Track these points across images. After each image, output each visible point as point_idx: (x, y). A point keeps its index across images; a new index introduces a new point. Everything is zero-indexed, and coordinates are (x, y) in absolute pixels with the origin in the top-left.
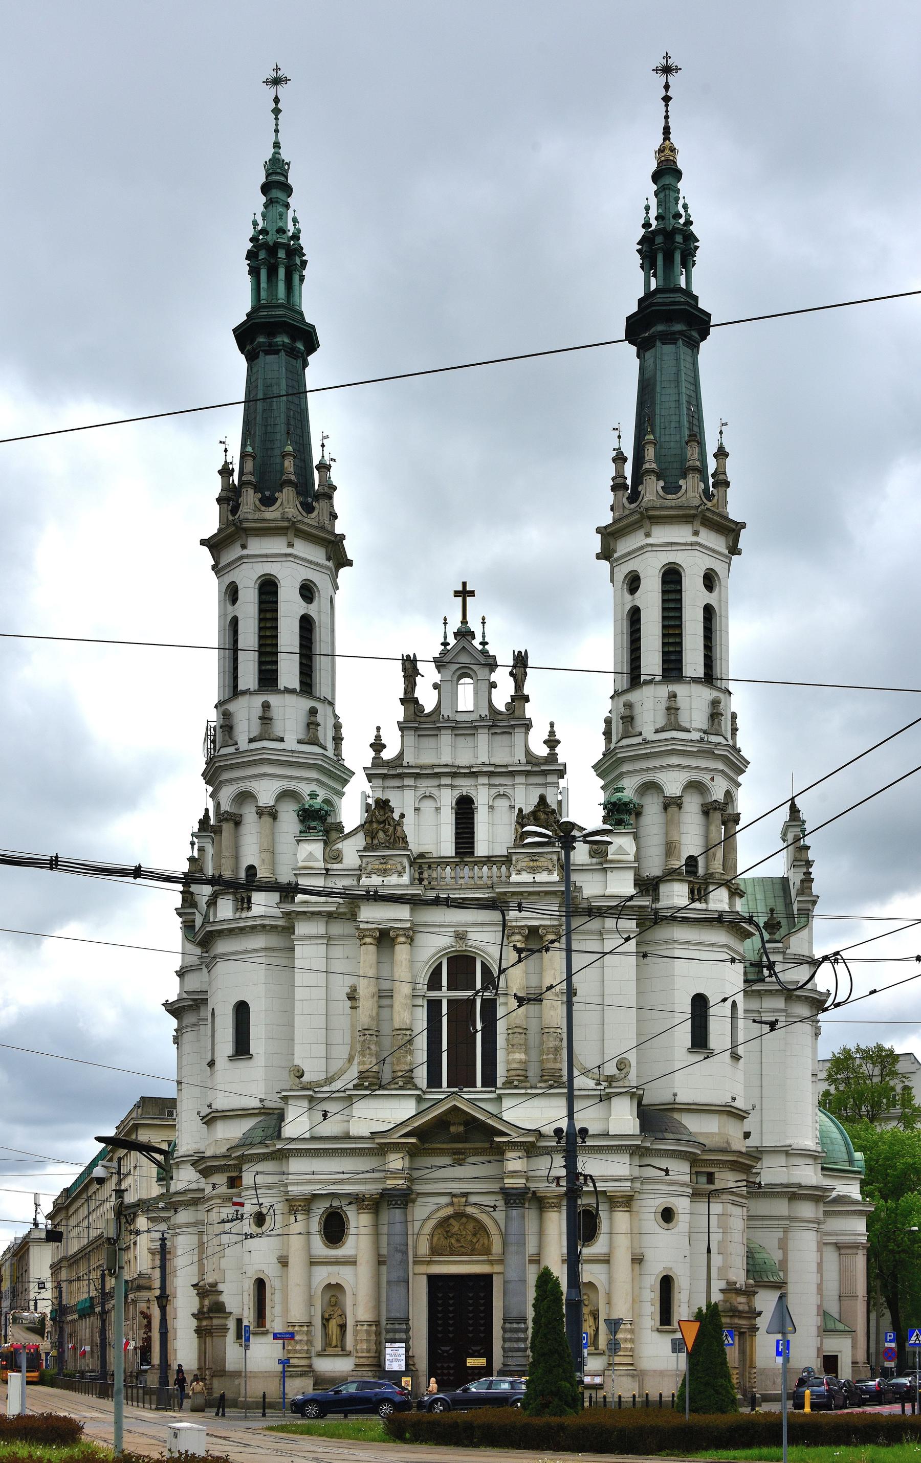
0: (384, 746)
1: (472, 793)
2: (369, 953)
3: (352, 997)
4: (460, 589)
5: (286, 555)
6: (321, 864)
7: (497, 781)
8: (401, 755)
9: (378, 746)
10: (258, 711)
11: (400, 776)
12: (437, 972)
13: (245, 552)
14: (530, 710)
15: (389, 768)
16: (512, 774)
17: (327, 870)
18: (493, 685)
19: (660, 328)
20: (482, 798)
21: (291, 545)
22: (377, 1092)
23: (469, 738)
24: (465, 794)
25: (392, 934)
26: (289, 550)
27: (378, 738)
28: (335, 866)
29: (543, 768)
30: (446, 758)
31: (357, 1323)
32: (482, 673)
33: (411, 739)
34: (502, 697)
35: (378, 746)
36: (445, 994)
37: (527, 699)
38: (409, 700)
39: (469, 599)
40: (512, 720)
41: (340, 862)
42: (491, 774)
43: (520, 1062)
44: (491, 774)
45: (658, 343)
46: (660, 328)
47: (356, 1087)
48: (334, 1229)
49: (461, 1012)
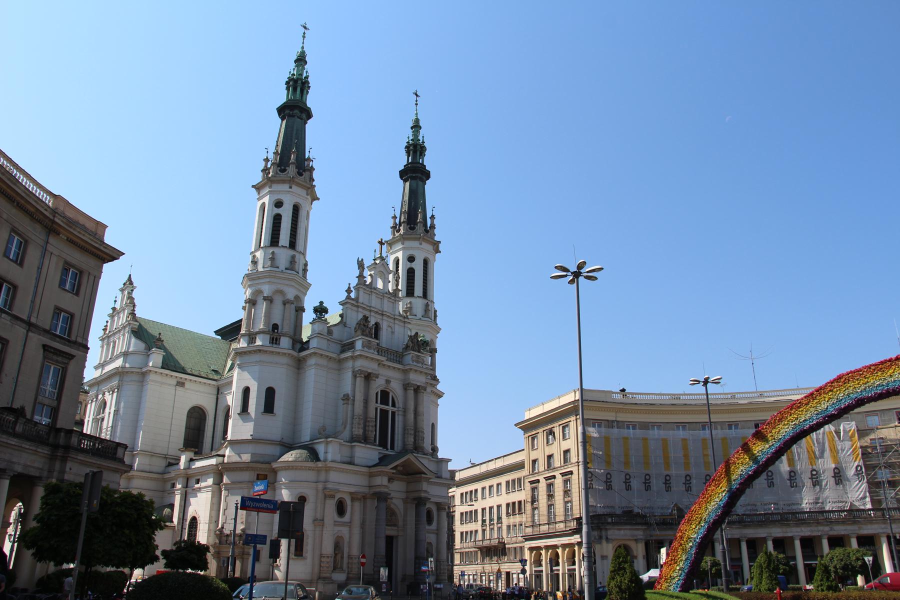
9: (349, 291)
10: (289, 259)
11: (358, 306)
27: (349, 288)
31: (350, 557)
34: (391, 287)
38: (361, 277)
48: (341, 509)
49: (384, 413)
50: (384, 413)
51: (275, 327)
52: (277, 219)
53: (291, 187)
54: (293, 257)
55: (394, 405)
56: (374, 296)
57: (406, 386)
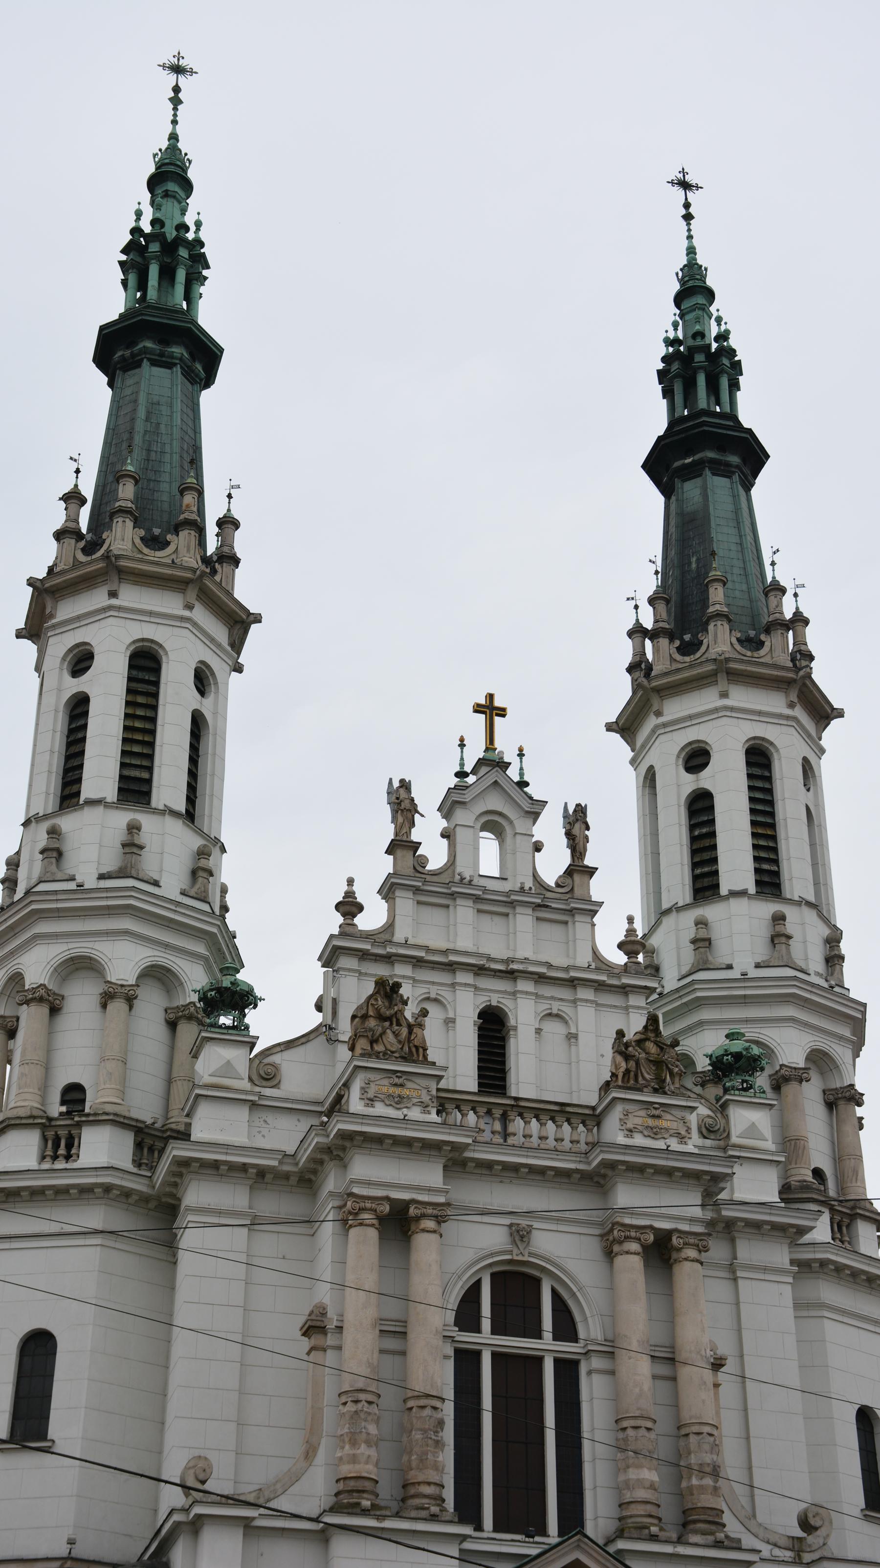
0: (360, 908)
1: (507, 1004)
2: (365, 1240)
3: (314, 1328)
4: (483, 702)
5: (182, 619)
6: (245, 1085)
7: (548, 991)
8: (390, 926)
9: (349, 907)
12: (472, 1295)
13: (114, 602)
14: (597, 888)
15: (374, 943)
16: (573, 983)
17: (261, 1096)
18: (538, 847)
19: (710, 454)
20: (523, 1013)
21: (189, 607)
22: (388, 1524)
23: (497, 920)
24: (494, 1003)
25: (413, 1211)
26: (187, 613)
27: (350, 894)
28: (268, 1092)
29: (626, 980)
30: (464, 942)
32: (520, 824)
33: (405, 903)
34: (552, 864)
35: (349, 907)
36: (486, 1339)
37: (591, 872)
38: (402, 845)
39: (497, 720)
40: (569, 900)
41: (276, 1086)
42: (540, 979)
43: (652, 1487)
44: (540, 979)
45: (707, 472)
46: (710, 454)
47: (334, 1509)
50: (518, 1372)
51: (74, 1094)
52: (79, 708)
53: (113, 594)
54: (133, 828)
55: (566, 1328)
56: (464, 912)
57: (611, 1241)
